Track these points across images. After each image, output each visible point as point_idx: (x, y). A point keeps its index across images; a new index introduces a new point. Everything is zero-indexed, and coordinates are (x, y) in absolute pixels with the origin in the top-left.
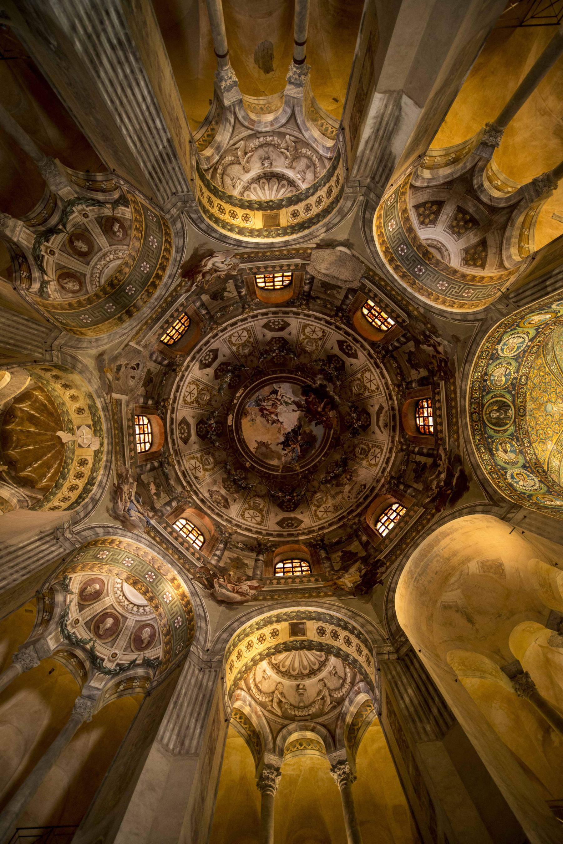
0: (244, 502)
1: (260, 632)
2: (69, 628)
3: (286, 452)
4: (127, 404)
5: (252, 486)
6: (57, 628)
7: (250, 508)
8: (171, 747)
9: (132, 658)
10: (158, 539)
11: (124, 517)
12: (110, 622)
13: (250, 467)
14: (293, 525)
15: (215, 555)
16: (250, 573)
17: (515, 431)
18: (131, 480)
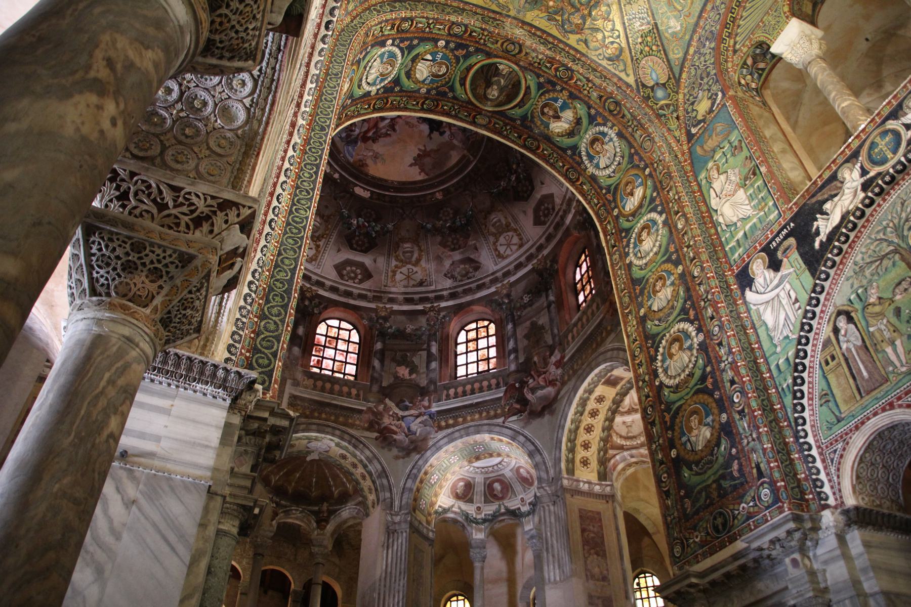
0: (486, 239)
1: (586, 413)
2: (479, 517)
3: (448, 133)
4: (296, 384)
5: (471, 210)
6: (472, 527)
7: (497, 236)
8: (558, 579)
9: (533, 493)
10: (451, 422)
11: (412, 442)
12: (497, 486)
13: (444, 196)
14: (548, 209)
15: (510, 353)
16: (550, 342)
17: (538, 76)
18: (381, 407)
